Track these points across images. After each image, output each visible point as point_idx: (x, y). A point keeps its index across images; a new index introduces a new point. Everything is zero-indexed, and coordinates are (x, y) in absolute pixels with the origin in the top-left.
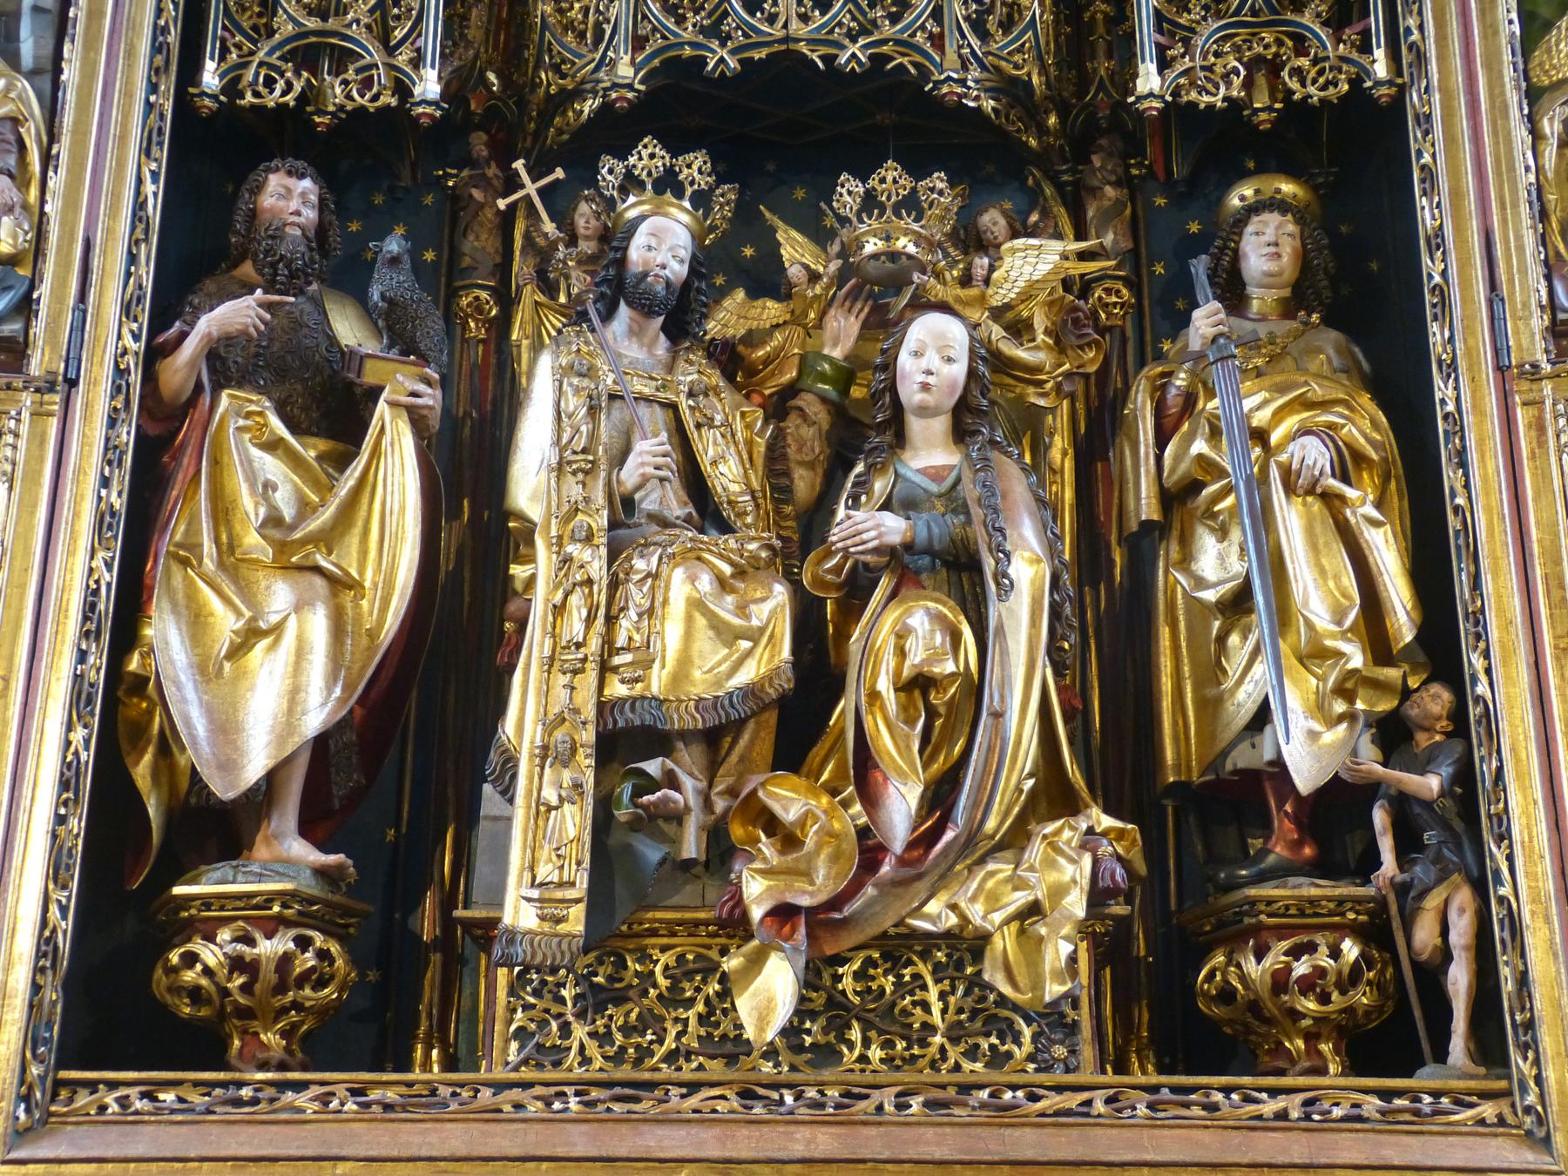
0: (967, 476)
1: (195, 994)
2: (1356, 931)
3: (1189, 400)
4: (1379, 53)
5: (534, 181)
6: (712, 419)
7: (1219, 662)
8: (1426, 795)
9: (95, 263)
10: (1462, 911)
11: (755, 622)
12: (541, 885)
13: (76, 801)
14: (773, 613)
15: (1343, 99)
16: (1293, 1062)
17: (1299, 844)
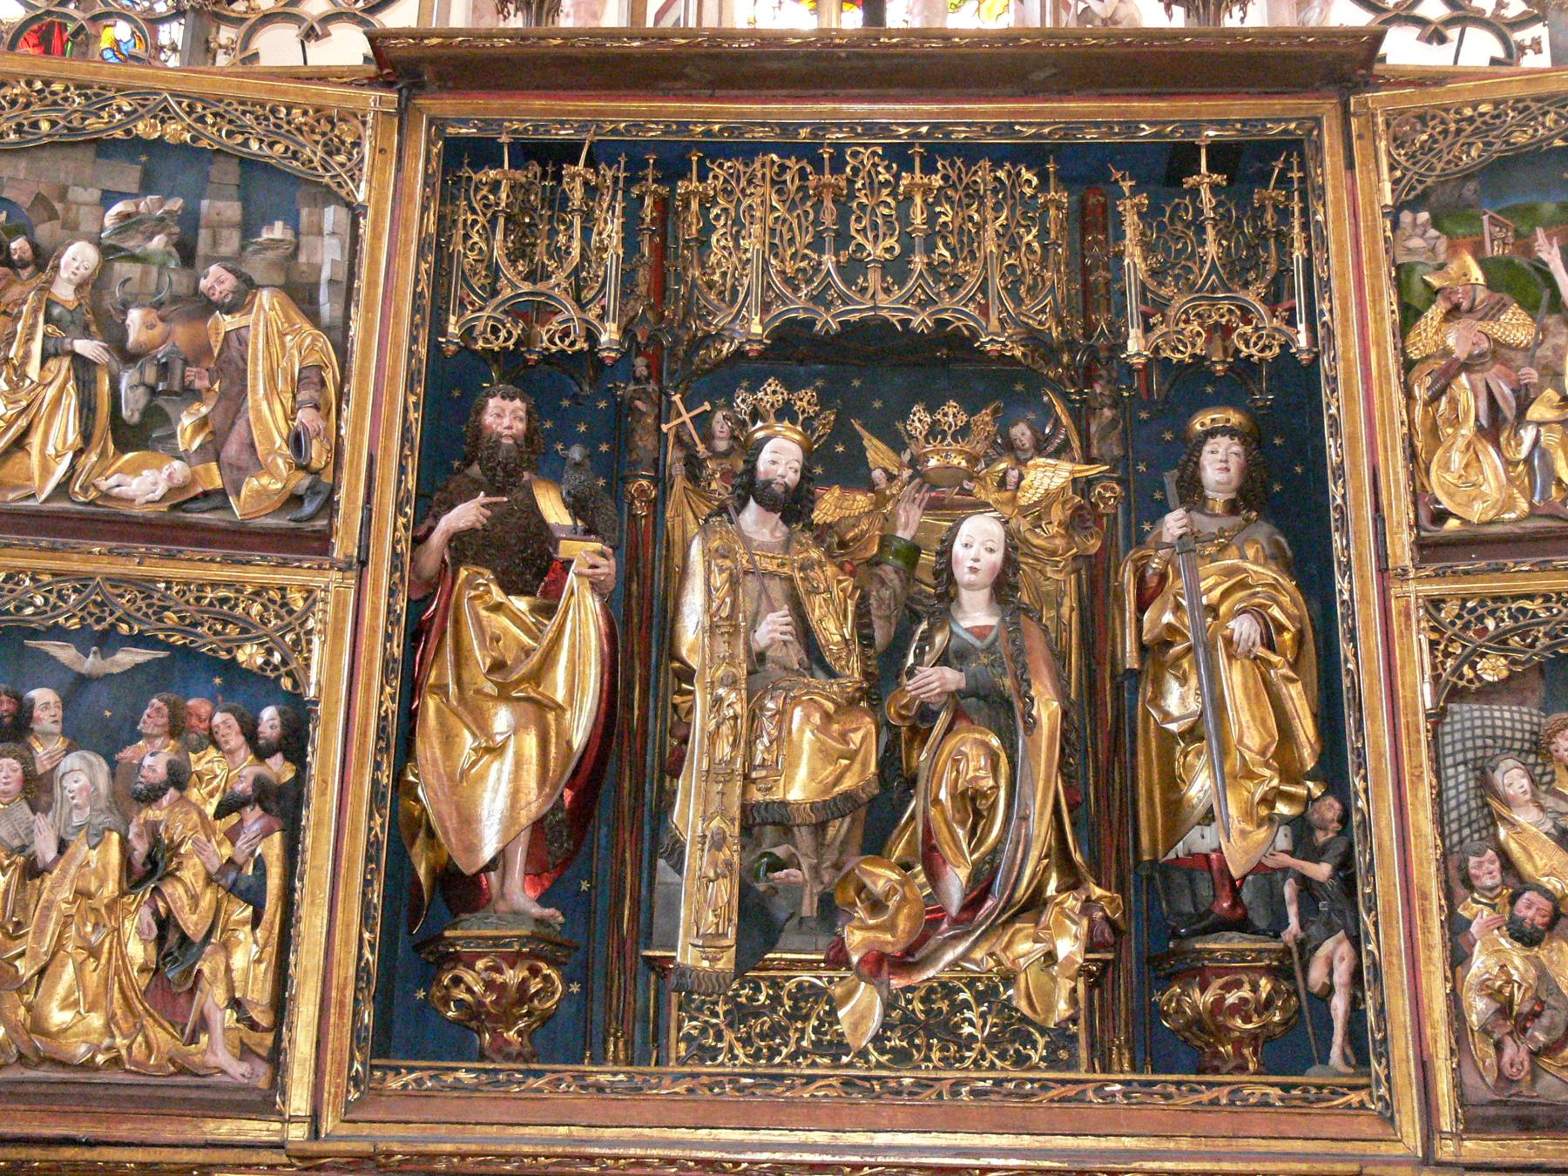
2: (1269, 971)
3: (1163, 577)
4: (1302, 327)
9: (378, 473)
10: (1343, 959)
12: (705, 935)
14: (864, 739)
16: (1225, 1062)
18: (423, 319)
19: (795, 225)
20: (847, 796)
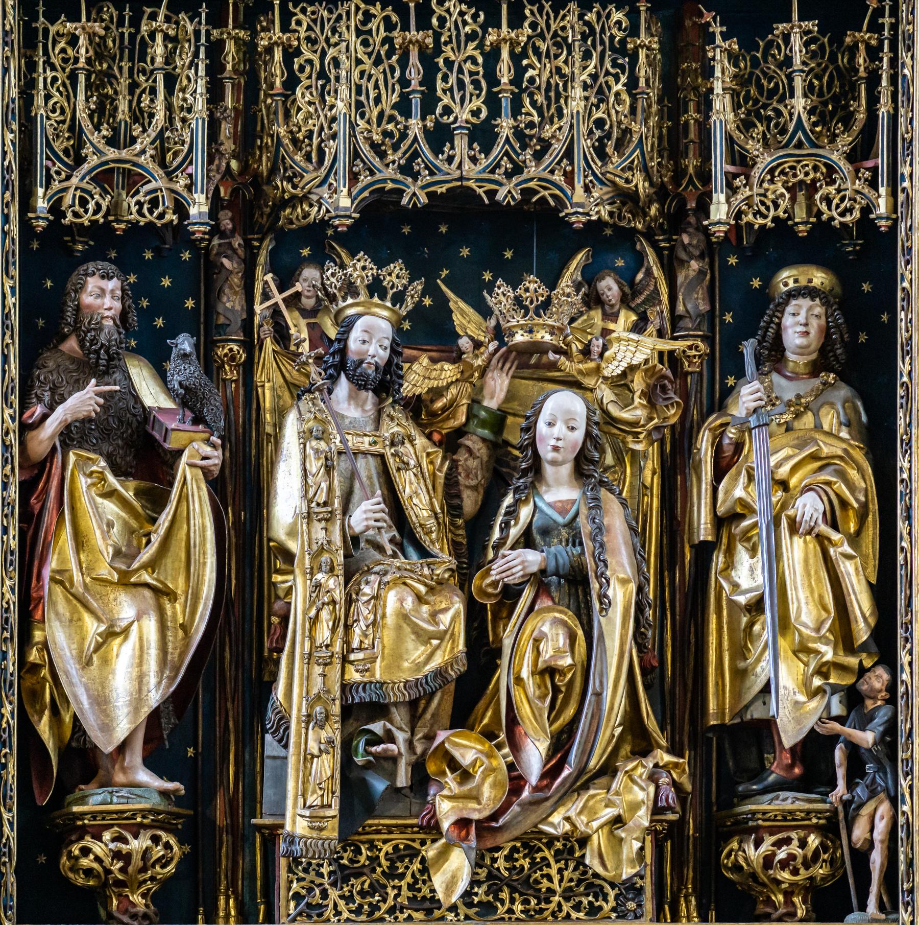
0: (584, 511)
1: (89, 872)
3: (738, 447)
5: (280, 292)
6: (408, 464)
7: (746, 645)
8: (865, 746)
11: (442, 627)
12: (310, 807)
13: (11, 754)
14: (453, 619)
15: (858, 222)
16: (776, 909)
17: (791, 767)
18: (13, 195)
19: (381, 83)
20: (440, 673)
